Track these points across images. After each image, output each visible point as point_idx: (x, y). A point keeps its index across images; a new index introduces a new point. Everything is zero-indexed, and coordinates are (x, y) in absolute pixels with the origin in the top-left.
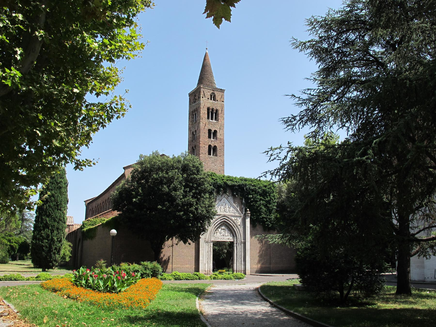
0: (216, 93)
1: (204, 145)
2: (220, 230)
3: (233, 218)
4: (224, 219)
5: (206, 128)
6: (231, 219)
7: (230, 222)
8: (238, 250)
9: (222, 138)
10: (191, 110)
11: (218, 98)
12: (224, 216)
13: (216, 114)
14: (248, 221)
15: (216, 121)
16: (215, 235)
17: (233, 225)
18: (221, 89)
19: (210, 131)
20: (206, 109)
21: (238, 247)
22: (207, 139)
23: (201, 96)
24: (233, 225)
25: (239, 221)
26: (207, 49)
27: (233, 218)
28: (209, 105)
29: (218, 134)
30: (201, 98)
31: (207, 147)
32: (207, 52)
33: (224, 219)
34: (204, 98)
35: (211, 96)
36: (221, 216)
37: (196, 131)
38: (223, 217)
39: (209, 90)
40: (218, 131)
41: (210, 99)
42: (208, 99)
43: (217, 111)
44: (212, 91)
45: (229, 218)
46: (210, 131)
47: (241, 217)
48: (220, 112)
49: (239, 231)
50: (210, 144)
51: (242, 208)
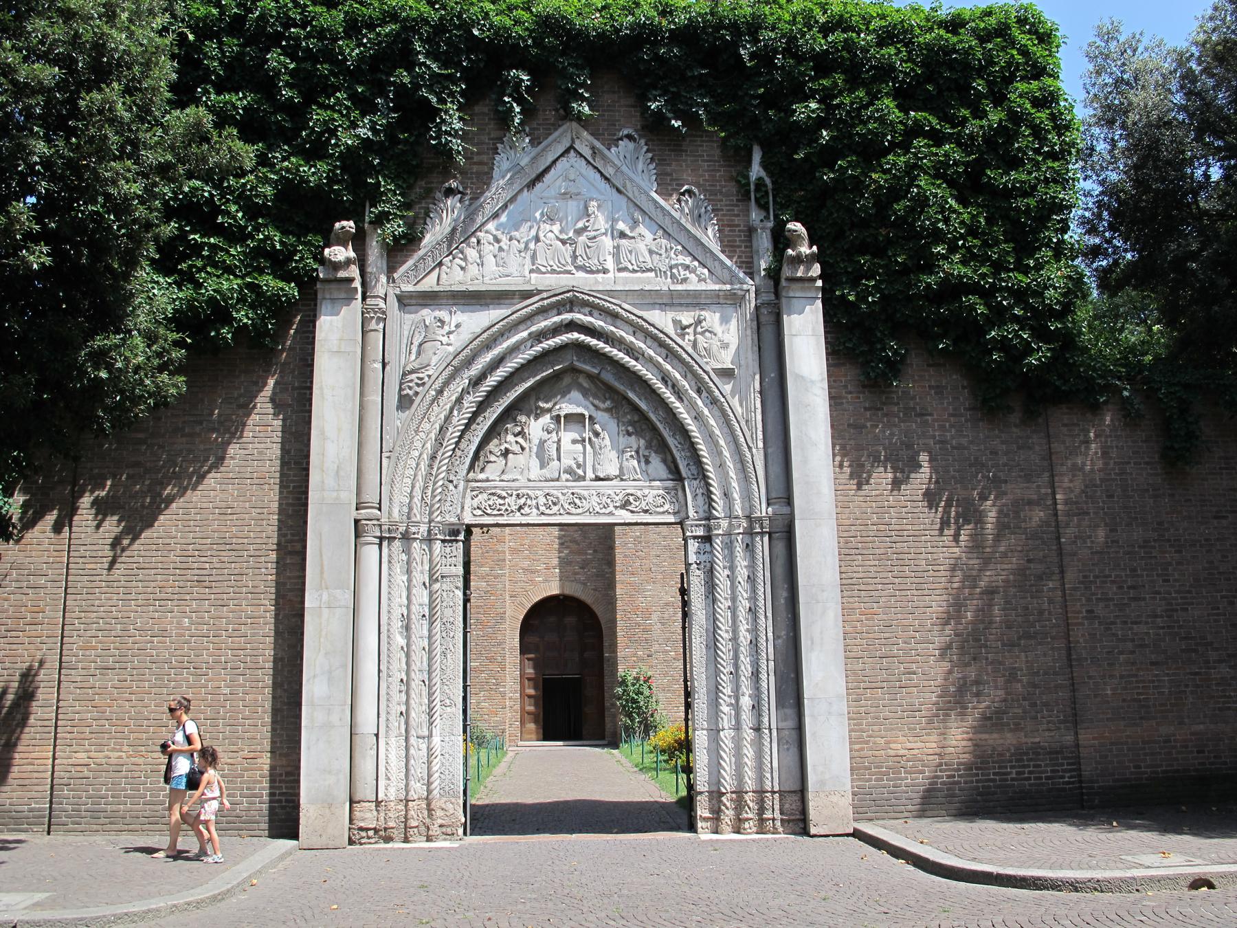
2: (536, 427)
3: (662, 320)
4: (571, 326)
6: (637, 329)
7: (630, 351)
8: (724, 604)
12: (572, 303)
14: (806, 332)
16: (492, 472)
17: (666, 379)
21: (722, 574)
24: (666, 379)
25: (724, 338)
27: (662, 320)
33: (571, 326)
36: (533, 304)
38: (559, 307)
45: (615, 316)
47: (735, 299)
49: (725, 429)
51: (751, 231)
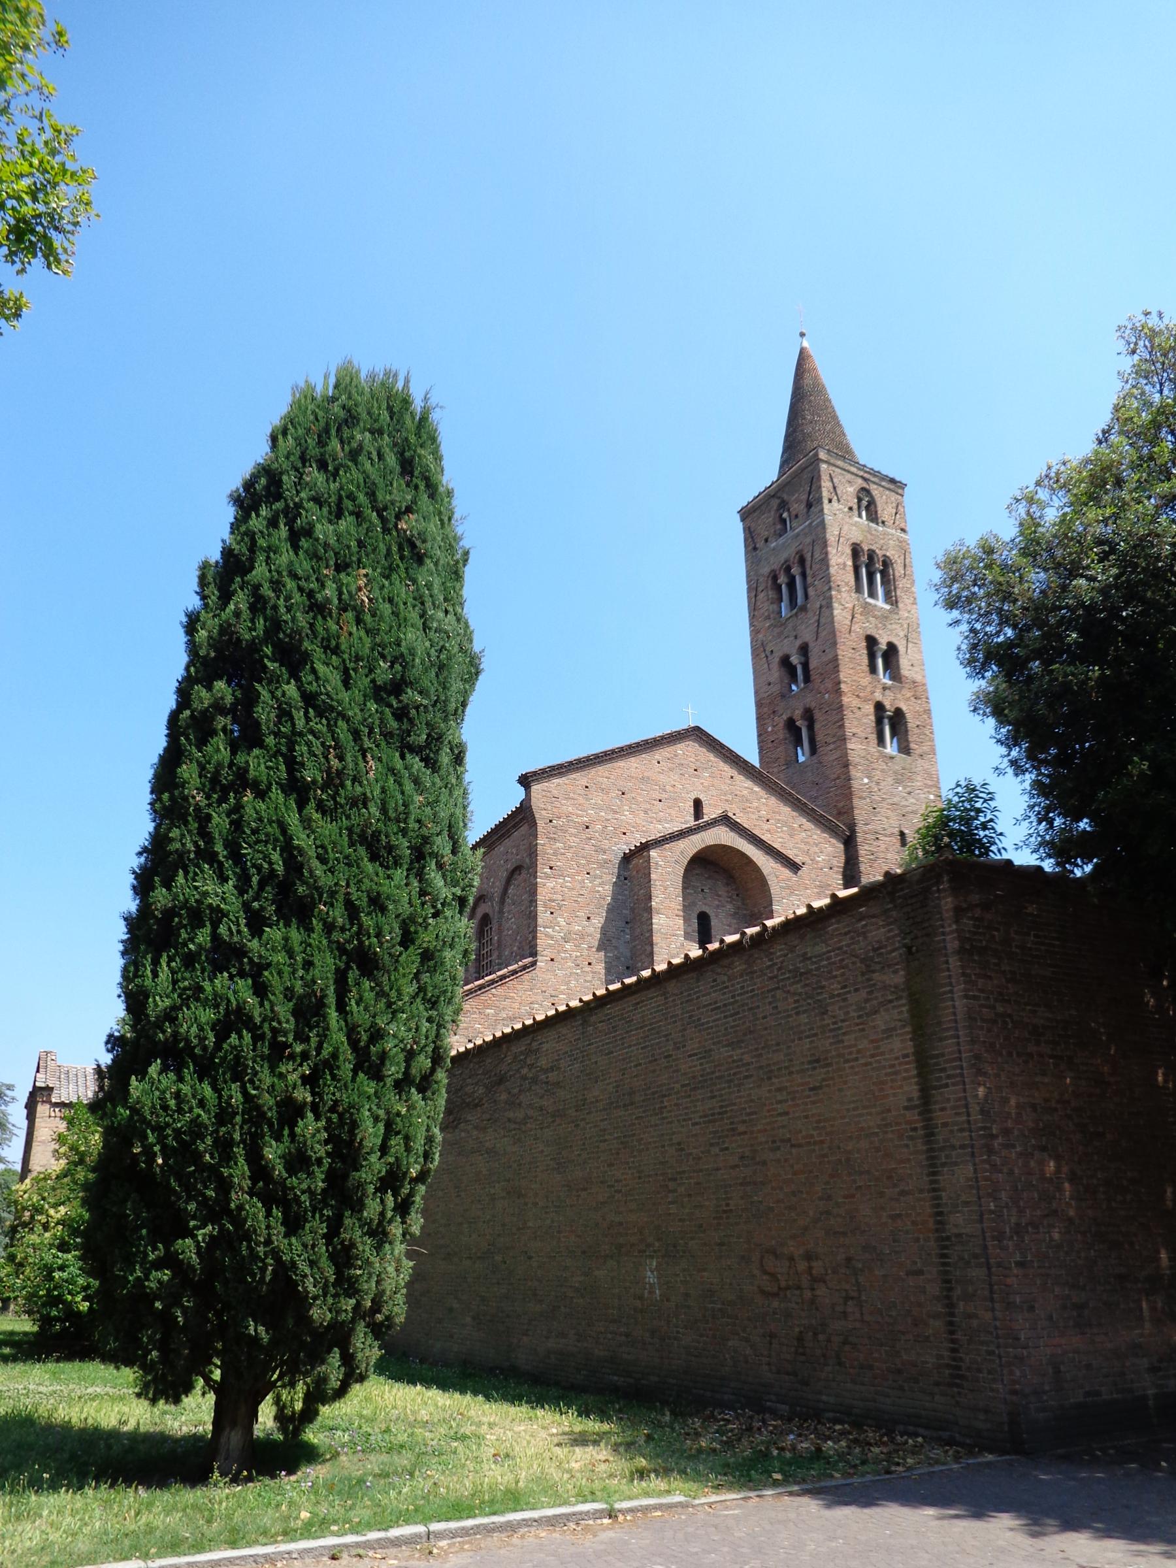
0: (876, 491)
1: (856, 703)
5: (856, 627)
9: (918, 678)
10: (766, 570)
11: (885, 510)
13: (884, 573)
15: (888, 607)
18: (893, 481)
19: (871, 641)
20: (849, 551)
22: (866, 679)
23: (825, 494)
26: (802, 335)
28: (856, 536)
29: (904, 662)
30: (826, 501)
31: (870, 709)
32: (805, 344)
34: (835, 503)
35: (860, 500)
37: (804, 650)
39: (849, 476)
40: (901, 650)
41: (856, 513)
42: (851, 509)
43: (887, 563)
44: (860, 483)
46: (871, 641)
48: (898, 569)
50: (878, 696)
